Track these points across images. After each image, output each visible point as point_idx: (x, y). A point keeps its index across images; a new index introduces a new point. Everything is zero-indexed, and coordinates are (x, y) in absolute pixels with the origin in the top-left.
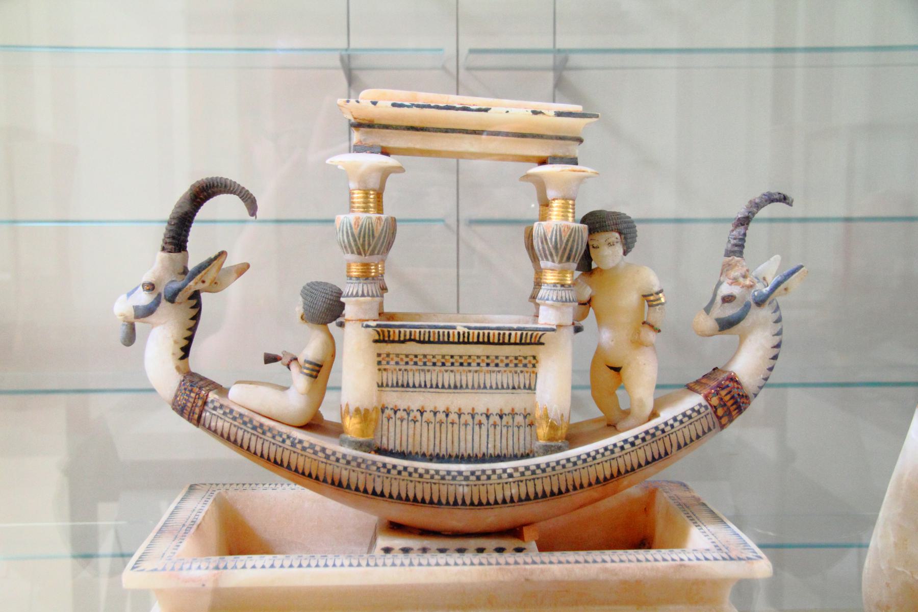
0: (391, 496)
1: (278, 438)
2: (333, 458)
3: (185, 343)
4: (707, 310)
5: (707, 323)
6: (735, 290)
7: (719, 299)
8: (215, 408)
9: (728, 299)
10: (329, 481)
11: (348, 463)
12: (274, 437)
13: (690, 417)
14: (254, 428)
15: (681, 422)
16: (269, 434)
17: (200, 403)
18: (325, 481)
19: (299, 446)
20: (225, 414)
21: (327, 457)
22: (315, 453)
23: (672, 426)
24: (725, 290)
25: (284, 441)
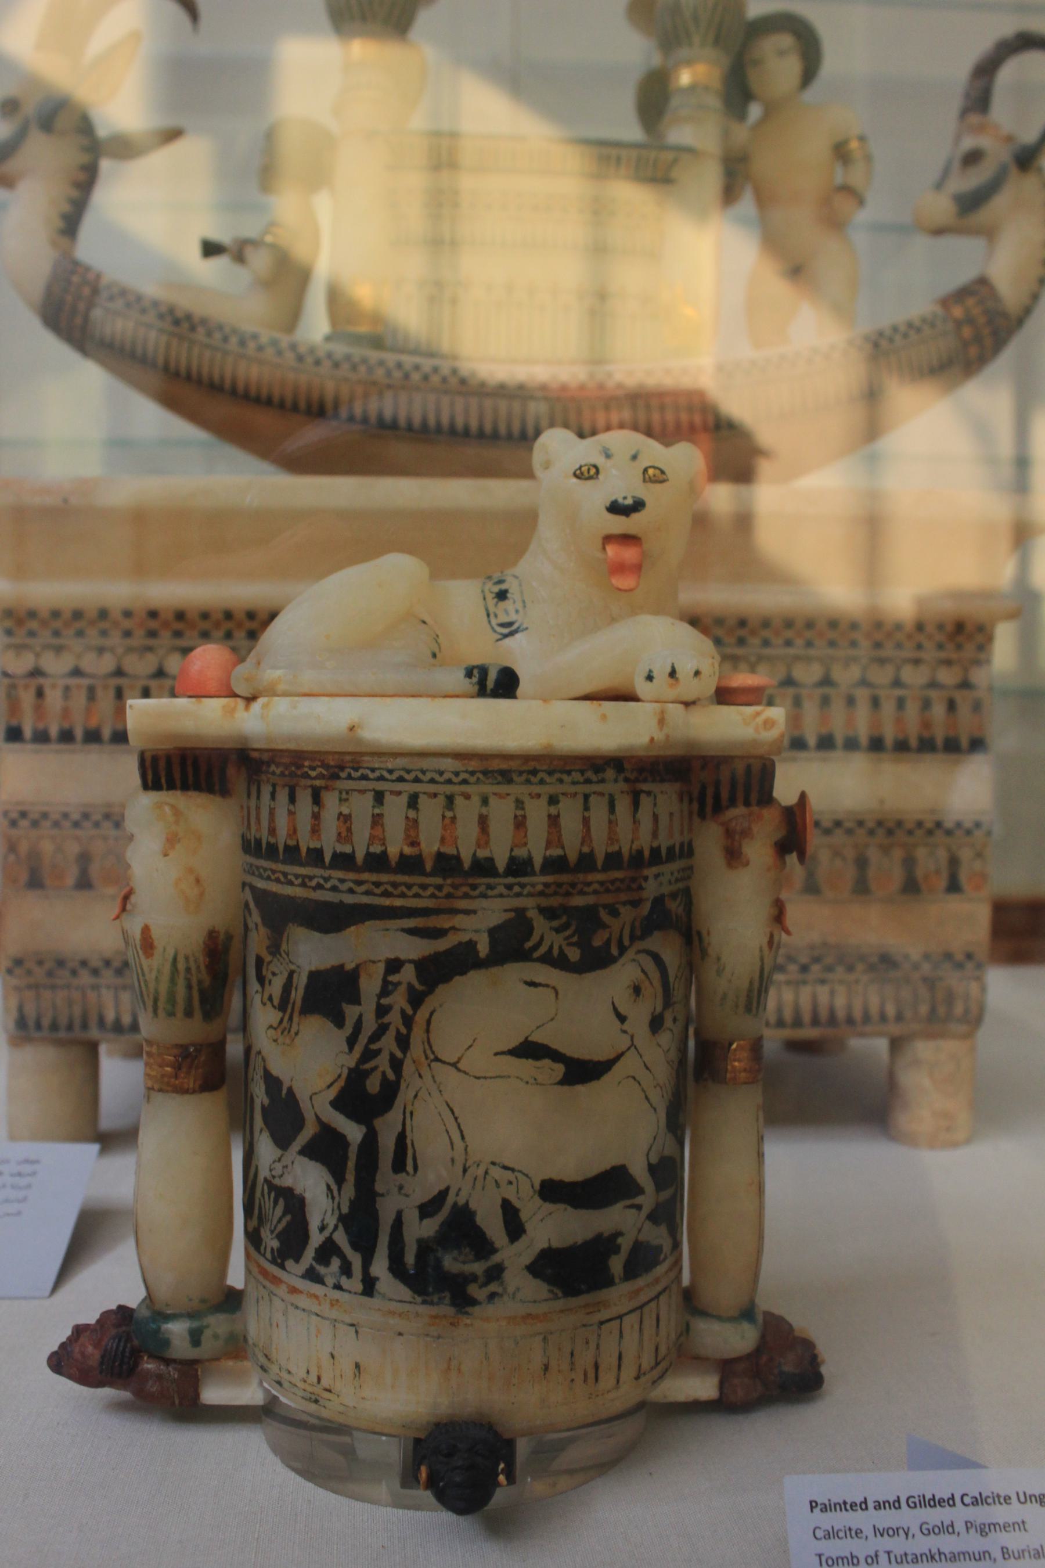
0: (410, 428)
1: (217, 336)
2: (310, 360)
3: (66, 208)
4: (939, 186)
5: (941, 207)
6: (984, 142)
7: (957, 164)
8: (111, 298)
9: (973, 158)
10: (302, 405)
11: (336, 365)
12: (209, 334)
13: (919, 330)
14: (177, 322)
15: (905, 336)
16: (201, 330)
17: (87, 291)
18: (295, 408)
19: (252, 345)
20: (128, 305)
21: (300, 359)
22: (280, 353)
23: (891, 340)
24: (969, 143)
25: (225, 339)
